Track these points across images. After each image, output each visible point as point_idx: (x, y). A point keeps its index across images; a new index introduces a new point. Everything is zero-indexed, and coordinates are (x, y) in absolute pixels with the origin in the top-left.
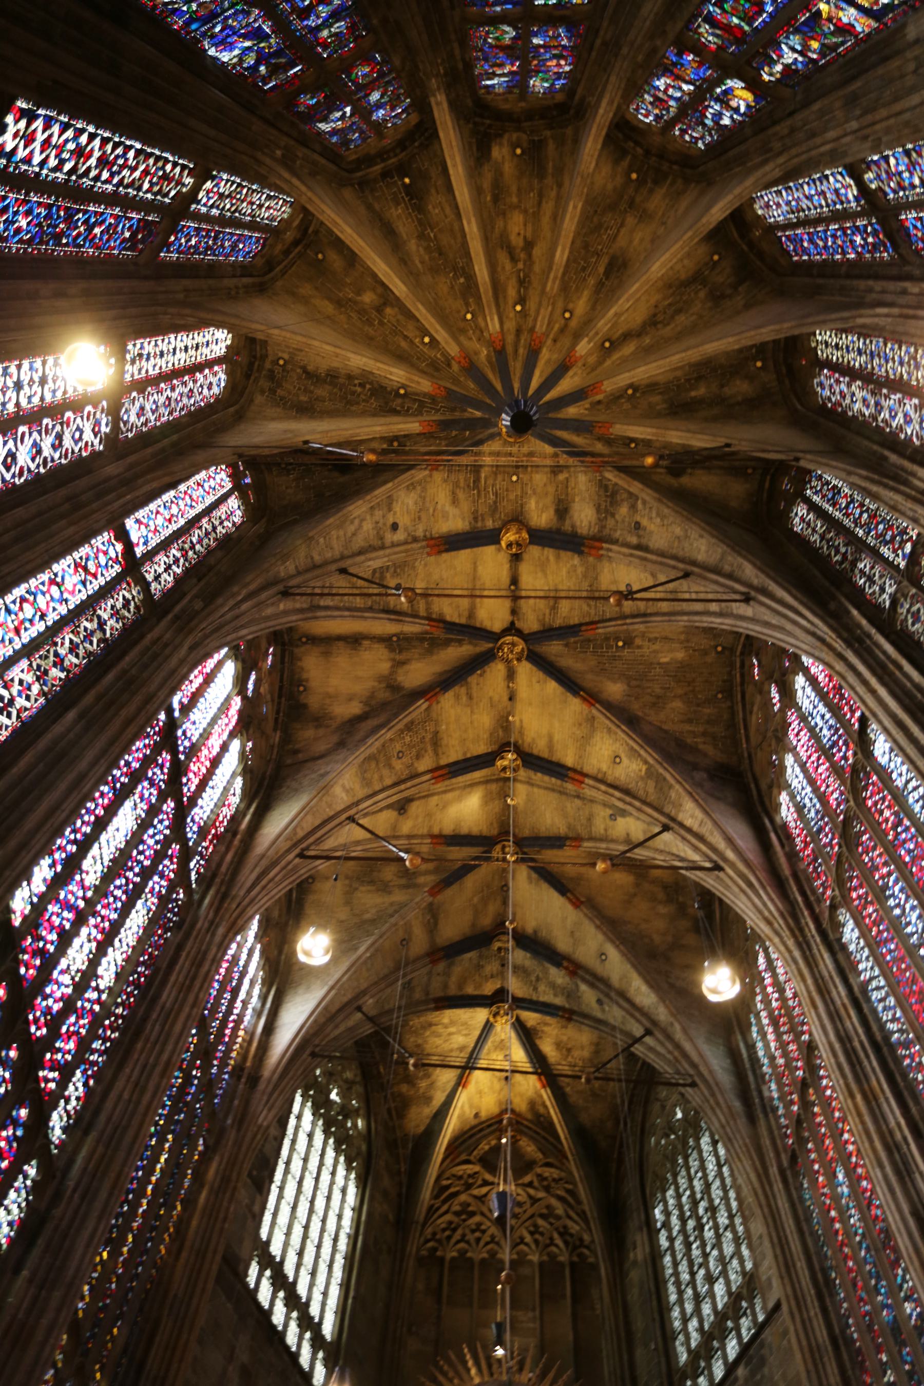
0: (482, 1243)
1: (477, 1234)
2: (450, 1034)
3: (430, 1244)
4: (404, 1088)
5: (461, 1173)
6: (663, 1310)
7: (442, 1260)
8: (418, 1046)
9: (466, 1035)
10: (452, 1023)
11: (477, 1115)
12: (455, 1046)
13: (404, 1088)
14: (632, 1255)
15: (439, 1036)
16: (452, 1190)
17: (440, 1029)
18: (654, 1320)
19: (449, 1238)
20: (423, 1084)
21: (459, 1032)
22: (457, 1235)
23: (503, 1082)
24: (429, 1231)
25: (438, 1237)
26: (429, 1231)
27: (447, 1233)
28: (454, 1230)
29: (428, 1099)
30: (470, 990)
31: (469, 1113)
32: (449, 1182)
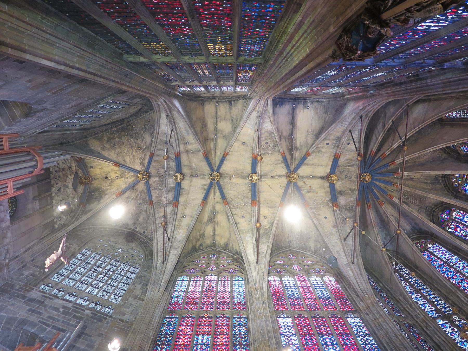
0: (56, 180)
1: (58, 177)
2: (129, 156)
4: (106, 138)
5: (72, 164)
8: (123, 143)
9: (130, 162)
10: (134, 156)
11: (92, 167)
12: (125, 158)
13: (106, 138)
15: (128, 151)
16: (67, 162)
17: (131, 151)
20: (108, 146)
21: (131, 159)
23: (105, 176)
29: (103, 149)
30: (153, 164)
31: (93, 165)
32: (69, 161)
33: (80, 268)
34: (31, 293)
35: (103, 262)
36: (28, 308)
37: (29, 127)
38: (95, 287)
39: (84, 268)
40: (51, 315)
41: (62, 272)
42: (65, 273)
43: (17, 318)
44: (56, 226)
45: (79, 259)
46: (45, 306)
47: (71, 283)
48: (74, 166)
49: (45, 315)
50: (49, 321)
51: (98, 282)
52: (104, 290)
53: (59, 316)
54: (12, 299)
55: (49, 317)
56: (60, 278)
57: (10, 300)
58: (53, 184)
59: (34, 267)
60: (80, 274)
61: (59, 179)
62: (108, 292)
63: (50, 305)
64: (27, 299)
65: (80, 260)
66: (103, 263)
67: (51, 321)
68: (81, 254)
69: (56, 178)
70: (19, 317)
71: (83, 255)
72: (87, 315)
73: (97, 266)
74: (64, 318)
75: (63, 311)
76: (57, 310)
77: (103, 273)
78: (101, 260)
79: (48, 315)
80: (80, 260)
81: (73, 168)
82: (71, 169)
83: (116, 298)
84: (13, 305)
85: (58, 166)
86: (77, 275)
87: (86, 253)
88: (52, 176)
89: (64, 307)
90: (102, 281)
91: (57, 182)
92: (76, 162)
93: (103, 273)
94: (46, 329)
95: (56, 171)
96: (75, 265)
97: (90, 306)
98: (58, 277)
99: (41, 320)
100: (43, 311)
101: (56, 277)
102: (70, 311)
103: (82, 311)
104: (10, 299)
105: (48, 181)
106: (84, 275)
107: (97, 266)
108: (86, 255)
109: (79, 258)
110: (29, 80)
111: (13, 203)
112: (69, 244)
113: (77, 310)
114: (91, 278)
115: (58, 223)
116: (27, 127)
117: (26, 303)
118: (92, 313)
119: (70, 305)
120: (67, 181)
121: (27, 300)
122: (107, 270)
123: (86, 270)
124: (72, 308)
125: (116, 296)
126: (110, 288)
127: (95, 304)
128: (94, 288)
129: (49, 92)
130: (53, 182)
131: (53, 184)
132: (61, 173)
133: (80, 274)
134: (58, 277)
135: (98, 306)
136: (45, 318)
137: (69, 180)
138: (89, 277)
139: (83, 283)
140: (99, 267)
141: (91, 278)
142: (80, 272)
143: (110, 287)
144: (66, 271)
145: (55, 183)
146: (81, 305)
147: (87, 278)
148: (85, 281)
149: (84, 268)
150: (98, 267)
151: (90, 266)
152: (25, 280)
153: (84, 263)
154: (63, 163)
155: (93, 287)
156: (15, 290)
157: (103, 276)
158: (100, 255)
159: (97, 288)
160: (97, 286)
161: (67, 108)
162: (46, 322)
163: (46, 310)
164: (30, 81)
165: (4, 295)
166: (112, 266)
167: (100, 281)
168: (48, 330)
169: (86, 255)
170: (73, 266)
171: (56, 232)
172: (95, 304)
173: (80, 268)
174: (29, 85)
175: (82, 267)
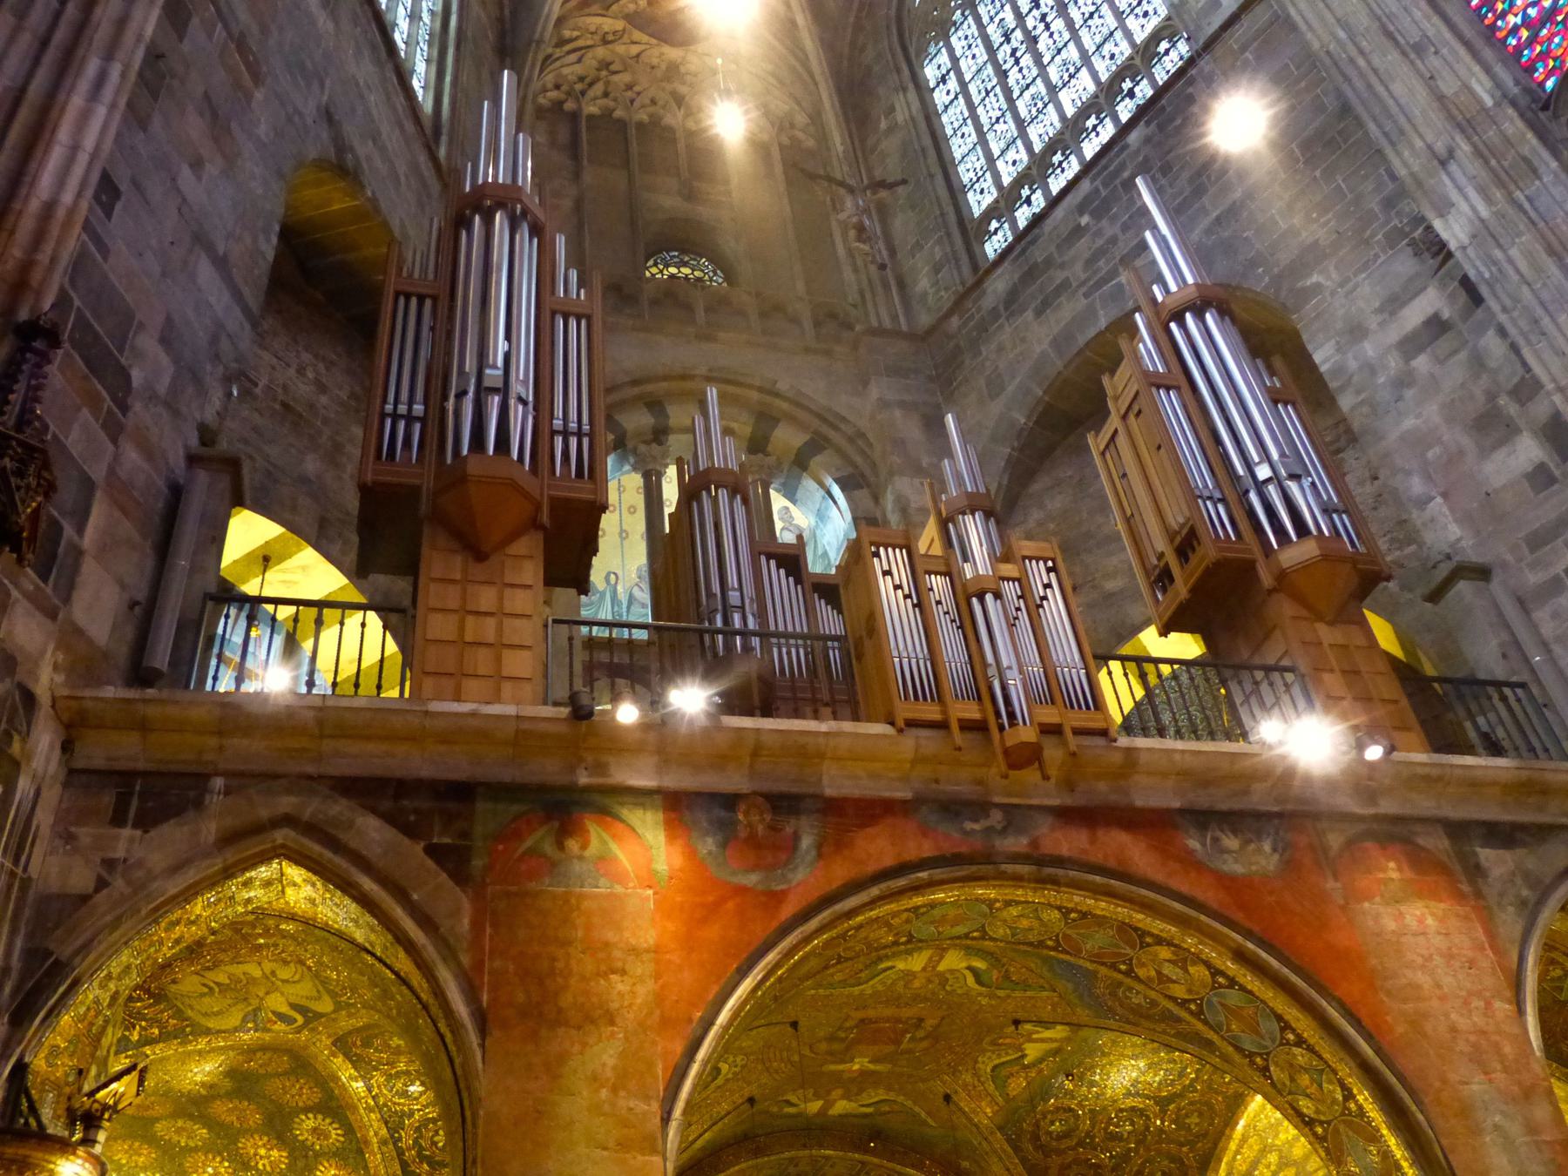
1: (629, 94)
3: (553, 94)
5: (592, 29)
6: (947, 167)
7: (574, 117)
14: (883, 125)
16: (580, 43)
18: (931, 176)
19: (583, 93)
22: (598, 89)
24: (549, 79)
25: (565, 88)
26: (549, 79)
27: (578, 87)
28: (591, 85)
32: (576, 33)
33: (981, 107)
34: (989, 291)
35: (997, 14)
36: (1029, 314)
37: (402, 169)
38: (1071, 76)
39: (987, 93)
40: (1087, 255)
41: (971, 174)
42: (978, 166)
43: (1042, 352)
44: (810, 143)
45: (952, 102)
46: (1048, 263)
47: (1017, 157)
48: (599, 20)
49: (1078, 272)
50: (1098, 270)
51: (1058, 59)
52: (1094, 48)
53: (1099, 233)
54: (983, 349)
55: (1090, 262)
56: (985, 185)
57: (984, 353)
58: (651, 116)
59: (913, 257)
60: (1003, 115)
61: (637, 88)
62: (1111, 34)
63: (1053, 248)
64: (1001, 308)
65: (956, 98)
66: (1001, 16)
67: (1101, 263)
68: (938, 85)
69: (632, 101)
70: (1045, 345)
71: (943, 80)
72: (1147, 140)
73: (1001, 44)
74: (1113, 219)
75: (1091, 214)
76: (1078, 231)
77: (1035, 28)
78: (985, 20)
79: (1078, 267)
80: (956, 98)
81: (606, 28)
82: (610, 38)
83: (1146, 14)
84: (1001, 349)
85: (588, 80)
86: (1000, 127)
87: (939, 67)
88: (618, 113)
89: (1081, 209)
90: (1060, 45)
91: (648, 101)
92: (587, 11)
93: (1035, 28)
94: (1120, 286)
95: (606, 95)
96: (964, 120)
97: (1124, 117)
98: (982, 192)
99: (1084, 289)
100: (1059, 276)
101: (979, 197)
102: (1104, 194)
103: (1125, 153)
104: (981, 354)
105: (633, 131)
106: (1011, 101)
107: (1001, 44)
108: (948, 72)
109: (947, 100)
110: (191, 166)
111: (682, 261)
112: (886, 118)
113: (1112, 168)
114: (1034, 79)
115: (800, 135)
116: (403, 179)
117: (1012, 314)
118: (1148, 123)
119: (1085, 186)
120: (655, 61)
121: (1006, 309)
122: (1031, 10)
123: (998, 89)
124: (1098, 182)
125: (1138, 10)
126: (1101, 21)
127: (1127, 100)
128: (1073, 81)
129: (249, 97)
130: (643, 116)
131: (651, 116)
132: (616, 78)
133: (1003, 115)
134: (982, 192)
135: (1137, 90)
136: (1083, 276)
137: (648, 53)
138: (1028, 86)
139: (1036, 117)
140: (1007, 37)
141: (1034, 79)
142: (999, 113)
143: (1096, 21)
144: (975, 159)
145: (651, 109)
146: (1106, 149)
147: (1027, 95)
148: (1036, 105)
149: (987, 93)
150: (1008, 40)
151: (989, 70)
152: (943, 293)
153: (972, 88)
154: (579, 61)
155: (1064, 86)
156: (960, 328)
157: (1016, 69)
158: (966, 18)
159: (1078, 70)
160: (1068, 70)
161: (330, 26)
162: (1096, 279)
163: (1062, 266)
164: (197, 165)
165: (963, 362)
166: (997, 20)
167: (1059, 51)
168: (1124, 281)
169: (948, 72)
170: (965, 129)
171: (828, 149)
172: (1127, 100)
173: (981, 107)
174: (212, 169)
175: (983, 100)
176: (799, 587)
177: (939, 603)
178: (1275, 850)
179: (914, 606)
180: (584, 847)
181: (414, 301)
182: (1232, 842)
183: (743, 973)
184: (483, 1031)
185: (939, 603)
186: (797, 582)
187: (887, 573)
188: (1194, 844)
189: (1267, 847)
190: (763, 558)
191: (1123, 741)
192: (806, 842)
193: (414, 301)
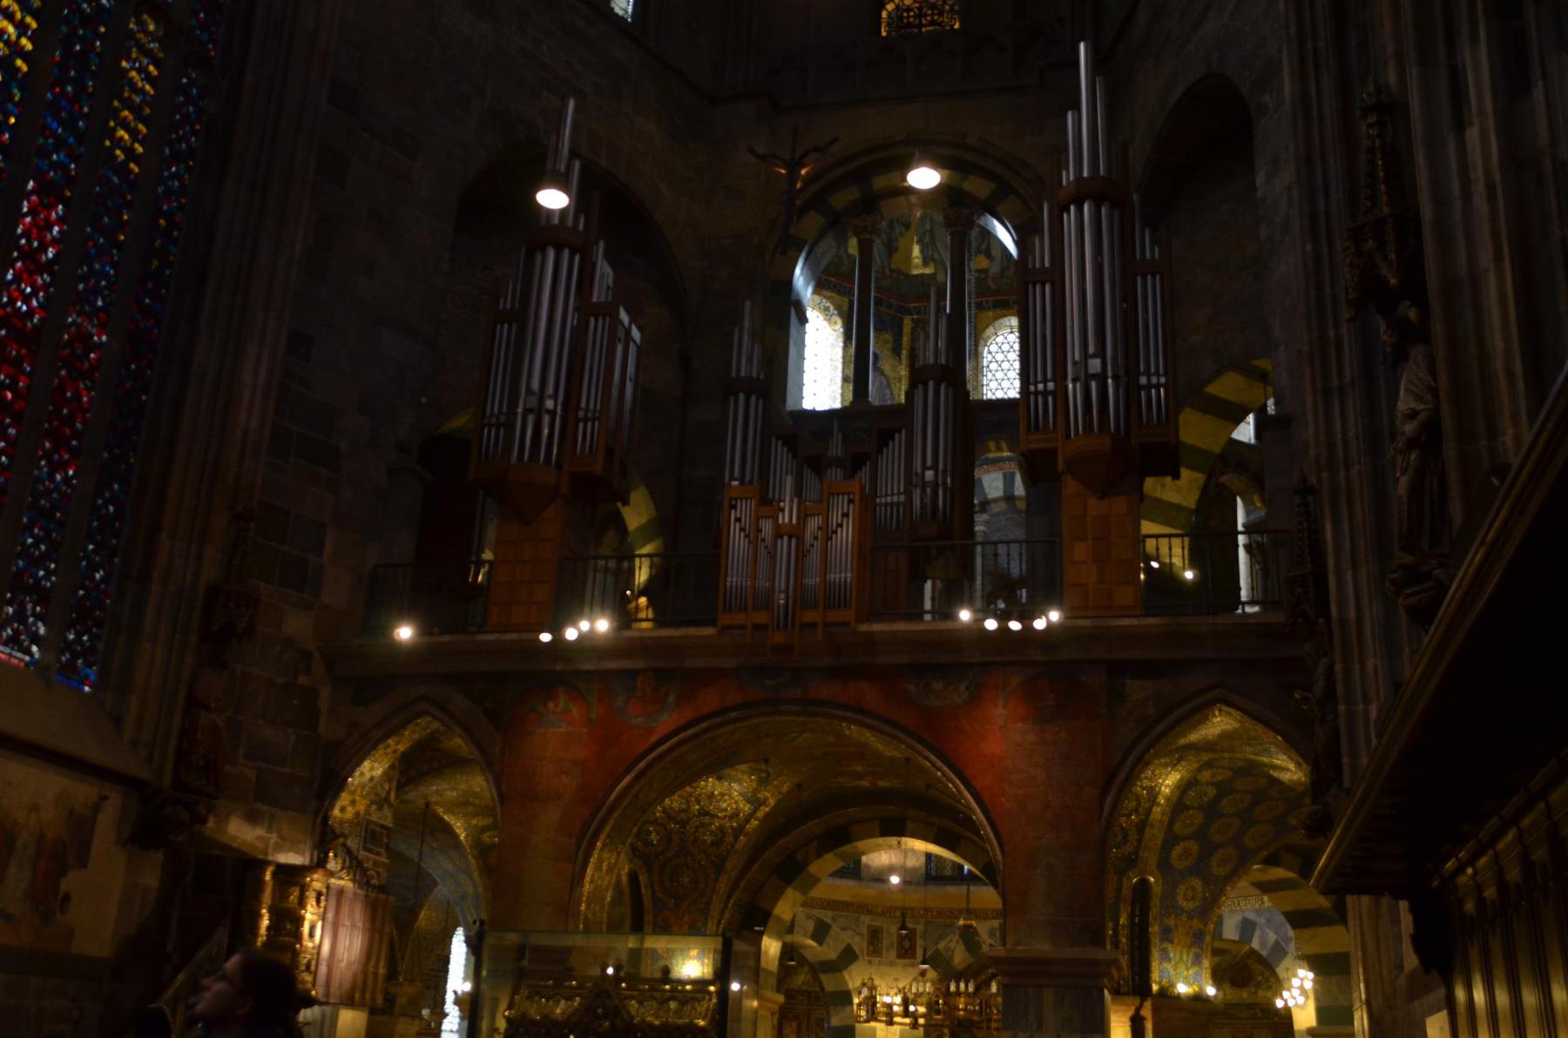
176: (795, 461)
177: (763, 540)
178: (967, 689)
179: (761, 531)
180: (556, 706)
181: (506, 326)
182: (938, 685)
183: (627, 772)
184: (502, 804)
185: (763, 540)
186: (794, 456)
187: (738, 520)
188: (911, 688)
189: (963, 687)
190: (774, 439)
191: (863, 628)
192: (672, 698)
193: (506, 326)
